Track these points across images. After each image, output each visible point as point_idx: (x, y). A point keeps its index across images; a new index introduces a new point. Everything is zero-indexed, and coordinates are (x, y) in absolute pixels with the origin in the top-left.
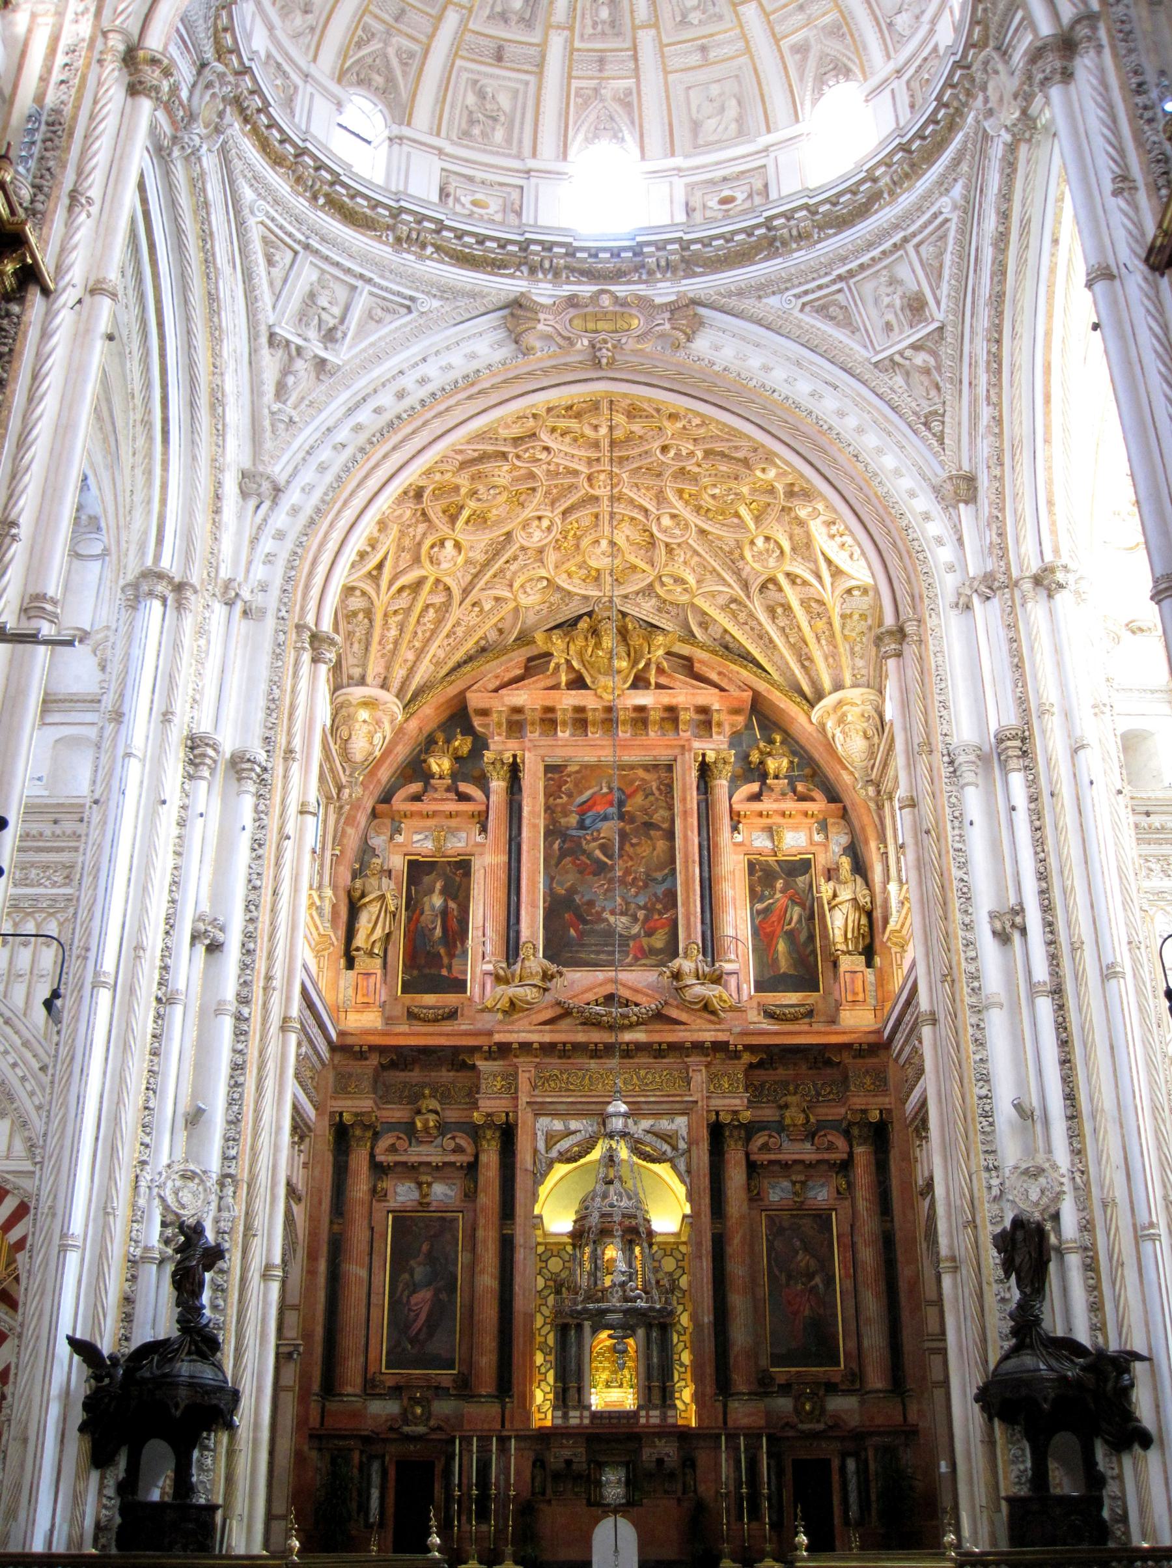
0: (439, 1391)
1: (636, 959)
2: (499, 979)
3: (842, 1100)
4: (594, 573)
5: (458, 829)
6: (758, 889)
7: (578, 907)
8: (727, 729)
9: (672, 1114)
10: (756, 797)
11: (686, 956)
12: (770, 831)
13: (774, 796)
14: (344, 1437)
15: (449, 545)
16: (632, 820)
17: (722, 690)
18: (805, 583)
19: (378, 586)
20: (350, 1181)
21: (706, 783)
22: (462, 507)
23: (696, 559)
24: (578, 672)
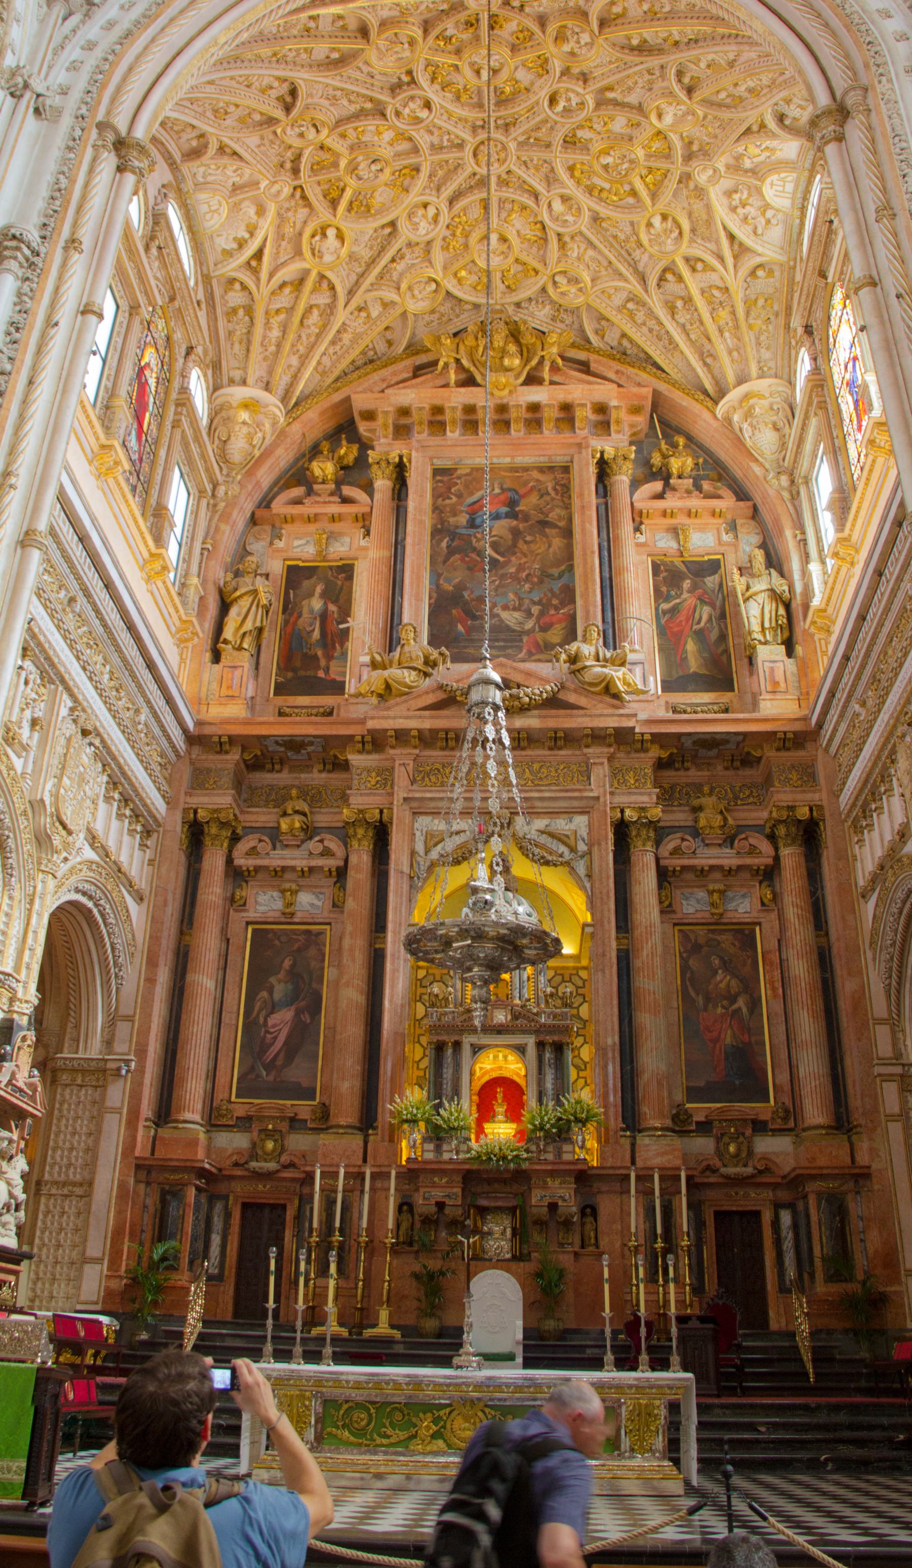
0: (295, 1123)
1: (530, 653)
2: (374, 665)
3: (760, 803)
4: (485, 280)
5: (341, 534)
6: (664, 589)
7: (466, 603)
8: (627, 431)
9: (570, 813)
10: (660, 496)
11: (585, 640)
12: (675, 531)
13: (678, 494)
14: (175, 1170)
15: (331, 233)
16: (526, 518)
17: (620, 386)
18: (708, 268)
19: (258, 279)
20: (202, 883)
21: (605, 487)
22: (343, 190)
23: (591, 253)
24: (467, 371)
